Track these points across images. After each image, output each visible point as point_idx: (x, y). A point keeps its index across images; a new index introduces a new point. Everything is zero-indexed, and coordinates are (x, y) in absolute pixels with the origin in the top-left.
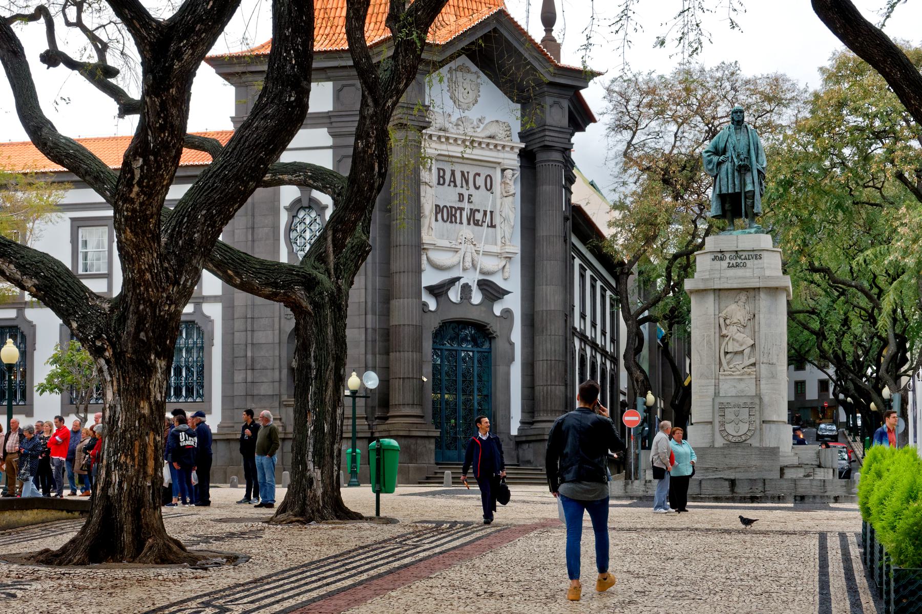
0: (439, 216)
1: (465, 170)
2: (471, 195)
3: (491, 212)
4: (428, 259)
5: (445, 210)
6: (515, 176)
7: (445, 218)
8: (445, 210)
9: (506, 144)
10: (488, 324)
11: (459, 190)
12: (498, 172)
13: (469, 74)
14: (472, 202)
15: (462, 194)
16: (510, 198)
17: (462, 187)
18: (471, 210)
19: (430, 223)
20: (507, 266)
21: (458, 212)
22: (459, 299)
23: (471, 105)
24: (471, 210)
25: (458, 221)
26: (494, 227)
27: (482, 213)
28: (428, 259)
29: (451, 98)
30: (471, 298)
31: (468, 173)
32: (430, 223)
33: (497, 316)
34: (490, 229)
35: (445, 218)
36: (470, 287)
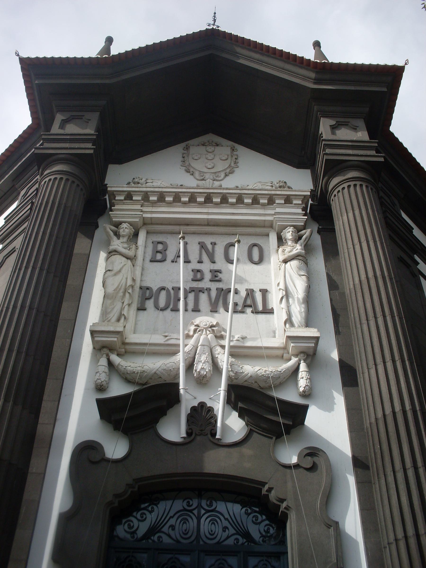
0: (150, 304)
1: (208, 241)
2: (220, 271)
3: (264, 292)
4: (110, 364)
5: (163, 294)
6: (304, 237)
7: (162, 302)
8: (163, 294)
9: (273, 192)
10: (263, 484)
11: (195, 265)
12: (273, 238)
13: (218, 149)
14: (220, 281)
15: (198, 271)
16: (295, 263)
17: (200, 262)
18: (220, 291)
19: (122, 309)
20: (303, 367)
21: (191, 296)
22: (184, 435)
23: (223, 175)
24: (220, 291)
25: (191, 305)
26: (271, 312)
27: (243, 294)
28: (110, 364)
29: (188, 171)
30: (214, 434)
31: (214, 244)
32: (122, 309)
33: (288, 467)
34: (262, 317)
35: (162, 302)
36: (210, 410)
